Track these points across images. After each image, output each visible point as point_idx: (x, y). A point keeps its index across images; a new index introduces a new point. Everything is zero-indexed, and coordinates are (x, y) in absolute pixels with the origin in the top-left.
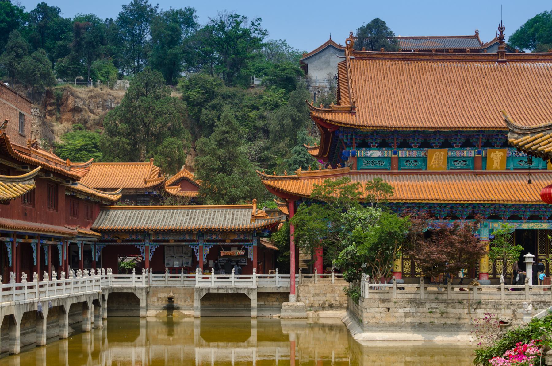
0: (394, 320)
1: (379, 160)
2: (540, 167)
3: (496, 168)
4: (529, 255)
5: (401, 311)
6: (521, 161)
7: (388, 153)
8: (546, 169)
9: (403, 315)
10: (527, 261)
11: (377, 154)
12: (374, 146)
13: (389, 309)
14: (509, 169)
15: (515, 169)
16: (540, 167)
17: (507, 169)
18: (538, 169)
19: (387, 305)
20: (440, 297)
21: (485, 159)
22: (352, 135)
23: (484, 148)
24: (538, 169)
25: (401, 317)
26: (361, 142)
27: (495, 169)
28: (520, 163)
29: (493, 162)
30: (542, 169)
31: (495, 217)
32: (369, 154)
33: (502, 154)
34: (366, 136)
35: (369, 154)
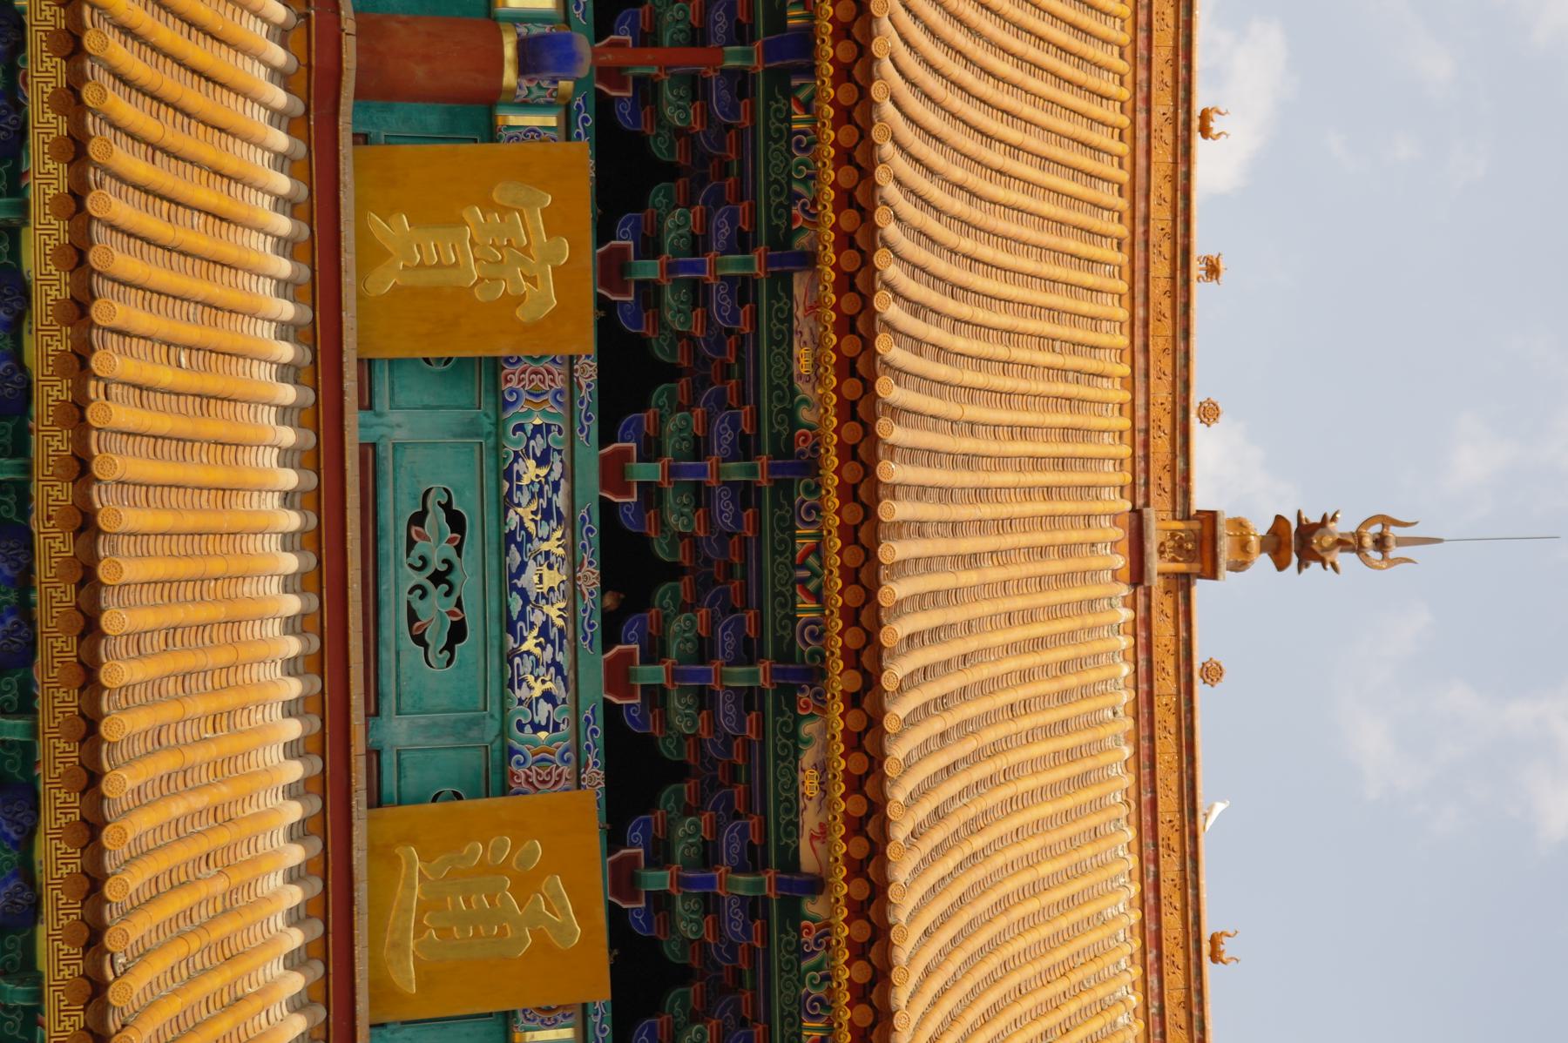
2: (397, 731)
3: (373, 254)
6: (456, 521)
8: (376, 800)
14: (367, 404)
15: (369, 451)
16: (397, 731)
17: (367, 366)
18: (374, 711)
21: (475, 113)
23: (586, 121)
24: (374, 711)
27: (363, 234)
28: (436, 519)
29: (438, 215)
30: (374, 754)
33: (542, 298)
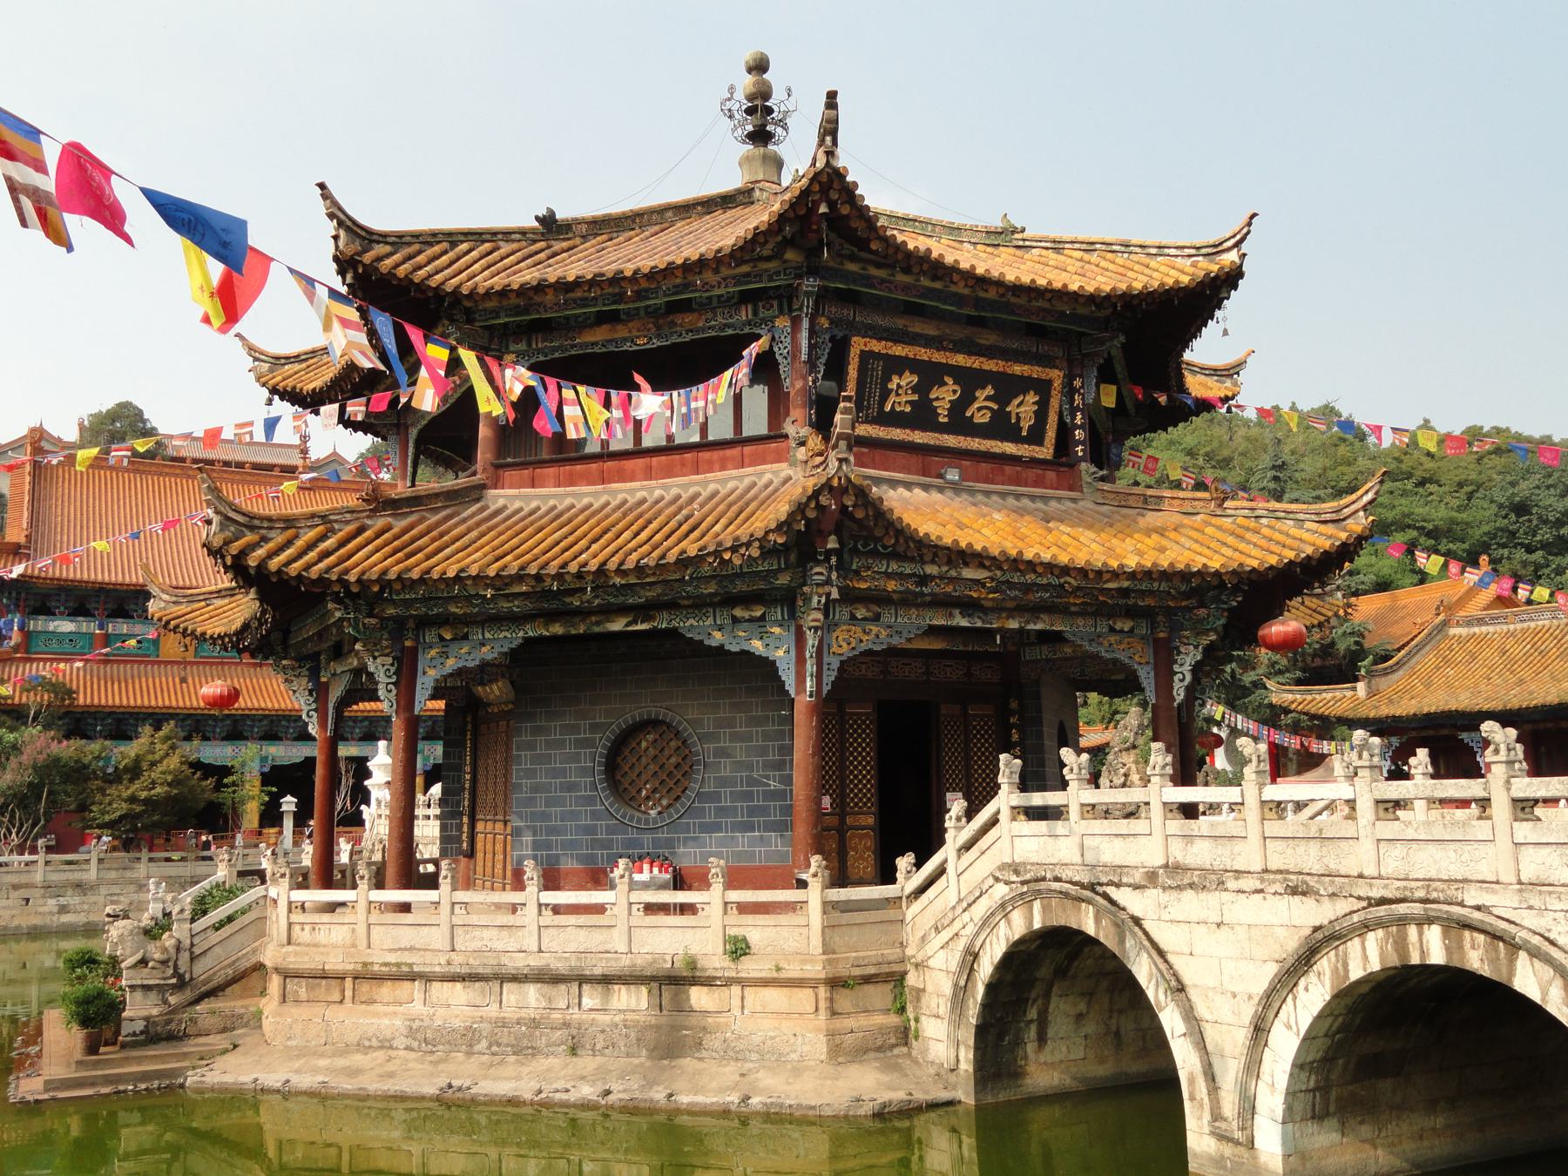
0: (36, 921)
1: (71, 638)
4: (289, 798)
5: (52, 902)
7: (89, 626)
9: (55, 909)
10: (284, 808)
11: (66, 626)
12: (62, 614)
13: (28, 900)
19: (24, 893)
20: (128, 874)
22: (19, 593)
25: (51, 913)
26: (38, 604)
31: (271, 736)
32: (52, 626)
34: (46, 596)
35: (52, 626)
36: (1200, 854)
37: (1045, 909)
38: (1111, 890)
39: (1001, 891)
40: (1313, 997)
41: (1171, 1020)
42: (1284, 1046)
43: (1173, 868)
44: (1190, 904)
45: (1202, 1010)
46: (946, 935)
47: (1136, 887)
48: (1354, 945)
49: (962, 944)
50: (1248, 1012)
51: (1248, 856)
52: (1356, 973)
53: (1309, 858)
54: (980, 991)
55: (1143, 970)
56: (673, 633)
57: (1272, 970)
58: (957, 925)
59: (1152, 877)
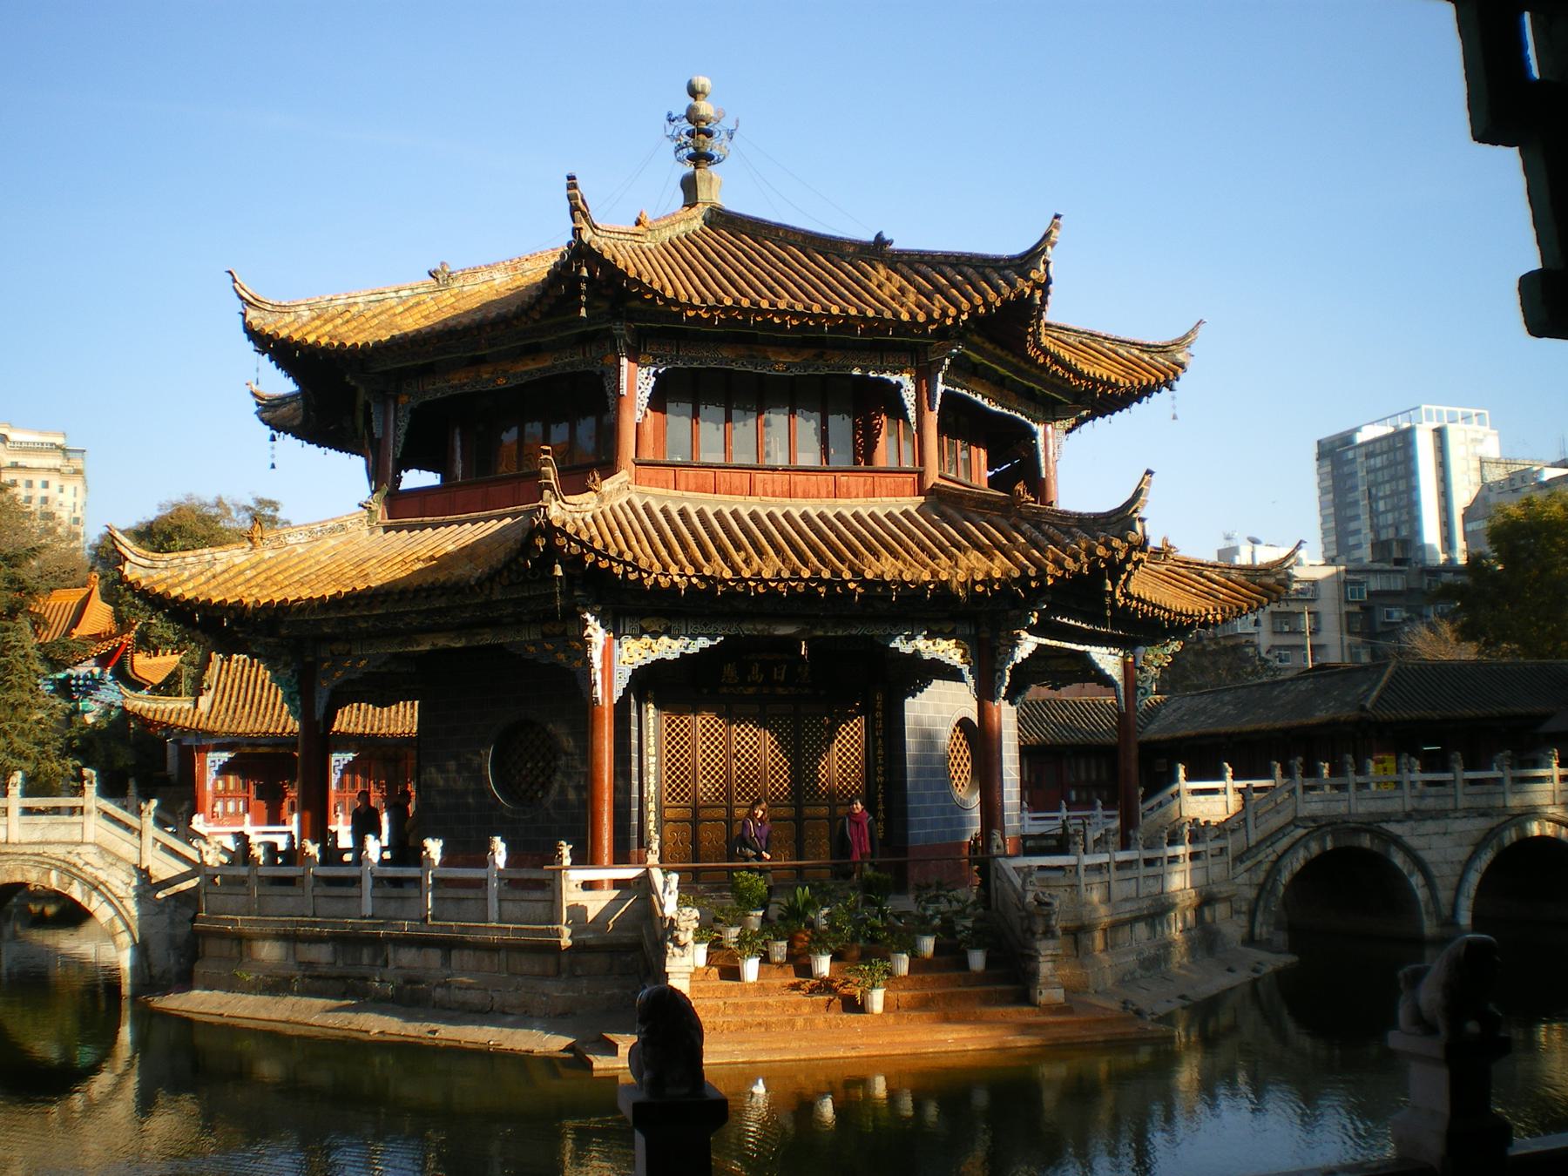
36: (1429, 803)
37: (1335, 839)
38: (1384, 825)
39: (1301, 832)
40: (1487, 857)
41: (1416, 881)
42: (1474, 878)
43: (1415, 810)
44: (1430, 826)
45: (1435, 871)
46: (1249, 864)
47: (1398, 821)
48: (1507, 834)
49: (1266, 866)
50: (1459, 869)
51: (1463, 802)
52: (1507, 842)
53: (1482, 802)
54: (1282, 889)
55: (1398, 859)
56: (1085, 654)
57: (1469, 849)
58: (1260, 857)
59: (1408, 816)
